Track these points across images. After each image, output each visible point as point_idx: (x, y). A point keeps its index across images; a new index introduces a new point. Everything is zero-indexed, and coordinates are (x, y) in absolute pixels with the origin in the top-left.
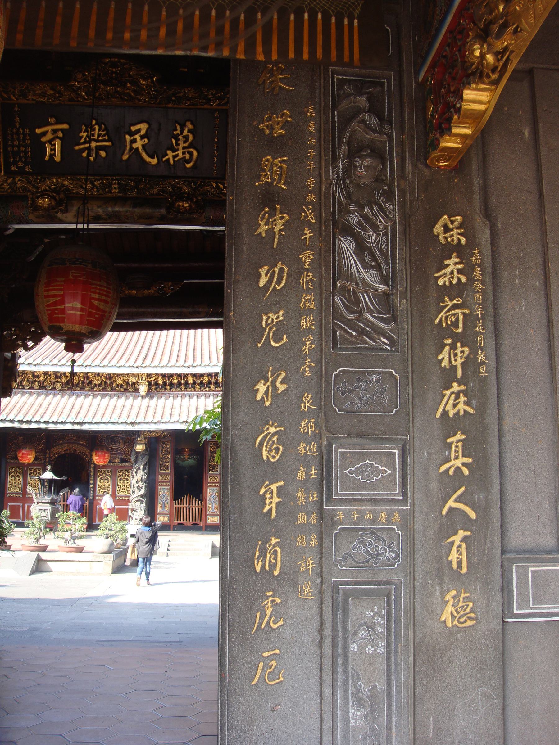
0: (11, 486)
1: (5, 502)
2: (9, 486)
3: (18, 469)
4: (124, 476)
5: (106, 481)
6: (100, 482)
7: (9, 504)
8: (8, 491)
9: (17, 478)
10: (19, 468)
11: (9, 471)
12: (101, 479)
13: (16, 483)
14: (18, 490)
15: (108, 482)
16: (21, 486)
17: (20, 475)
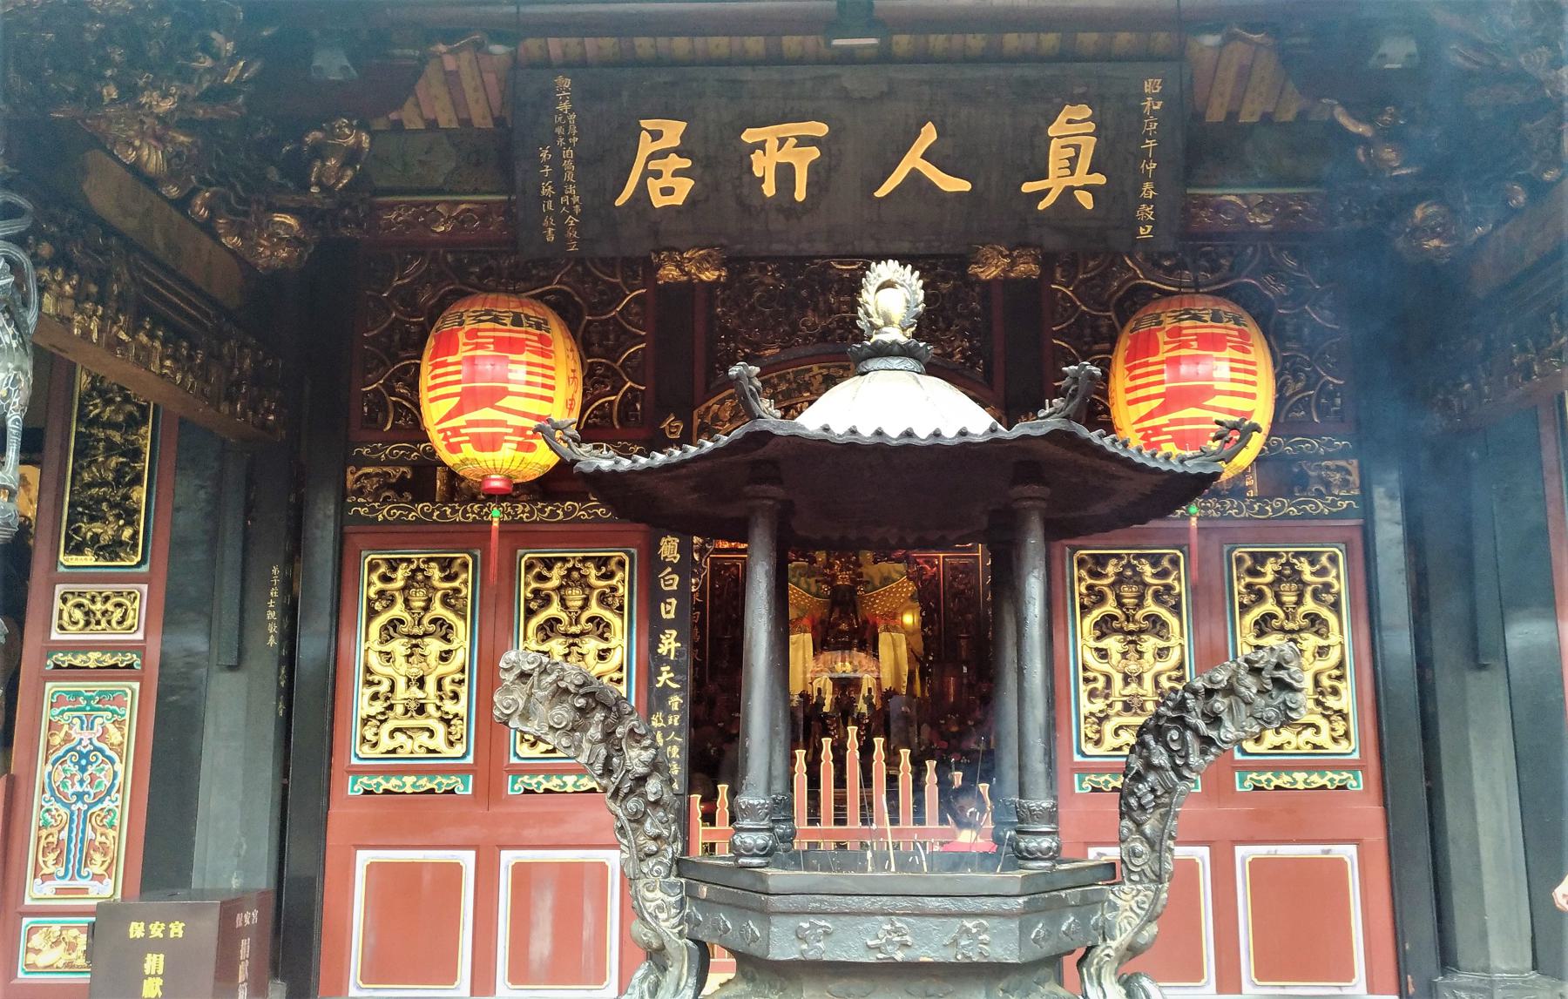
0: (379, 706)
1: (334, 838)
2: (363, 705)
3: (435, 573)
4: (1289, 598)
5: (1150, 643)
6: (1103, 654)
7: (364, 858)
8: (360, 753)
9: (434, 646)
10: (445, 565)
11: (371, 586)
12: (1105, 627)
13: (421, 682)
14: (439, 742)
15: (1161, 653)
16: (461, 708)
17: (449, 616)
